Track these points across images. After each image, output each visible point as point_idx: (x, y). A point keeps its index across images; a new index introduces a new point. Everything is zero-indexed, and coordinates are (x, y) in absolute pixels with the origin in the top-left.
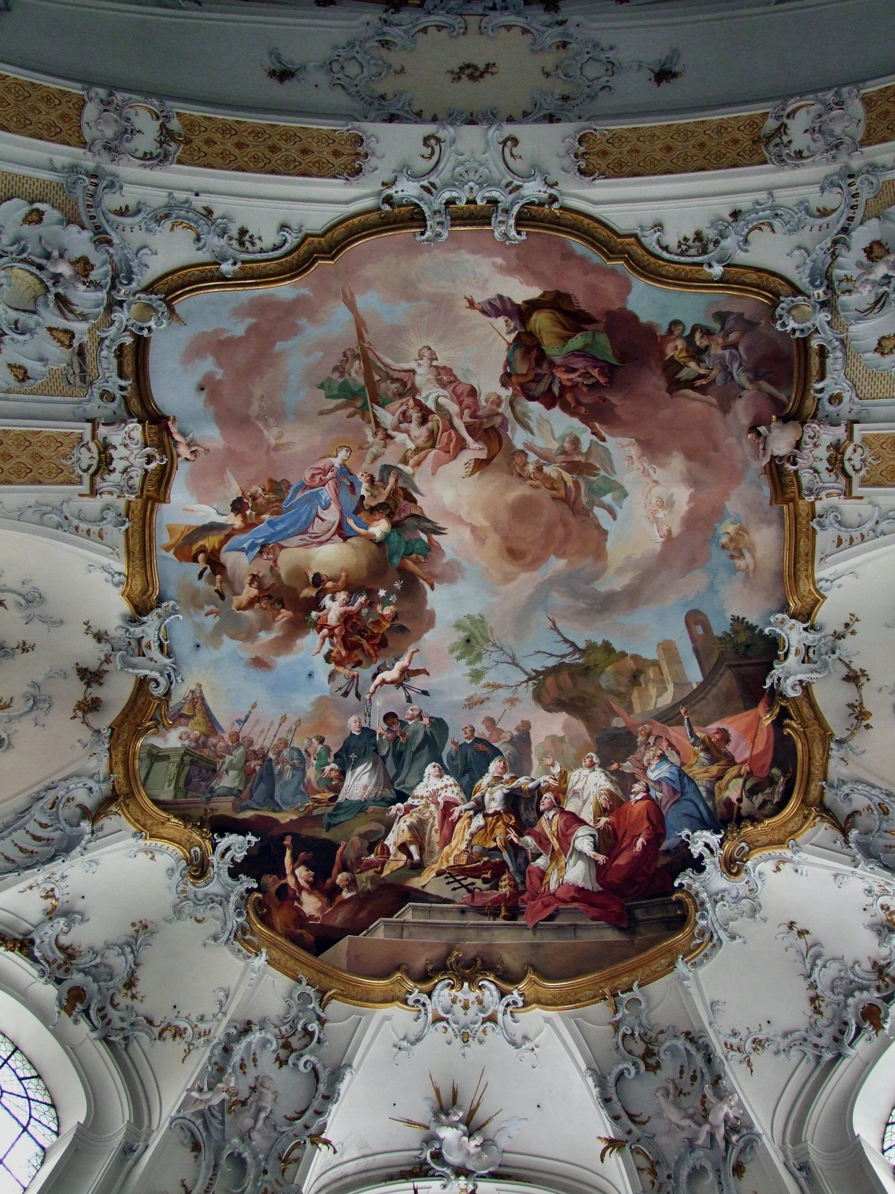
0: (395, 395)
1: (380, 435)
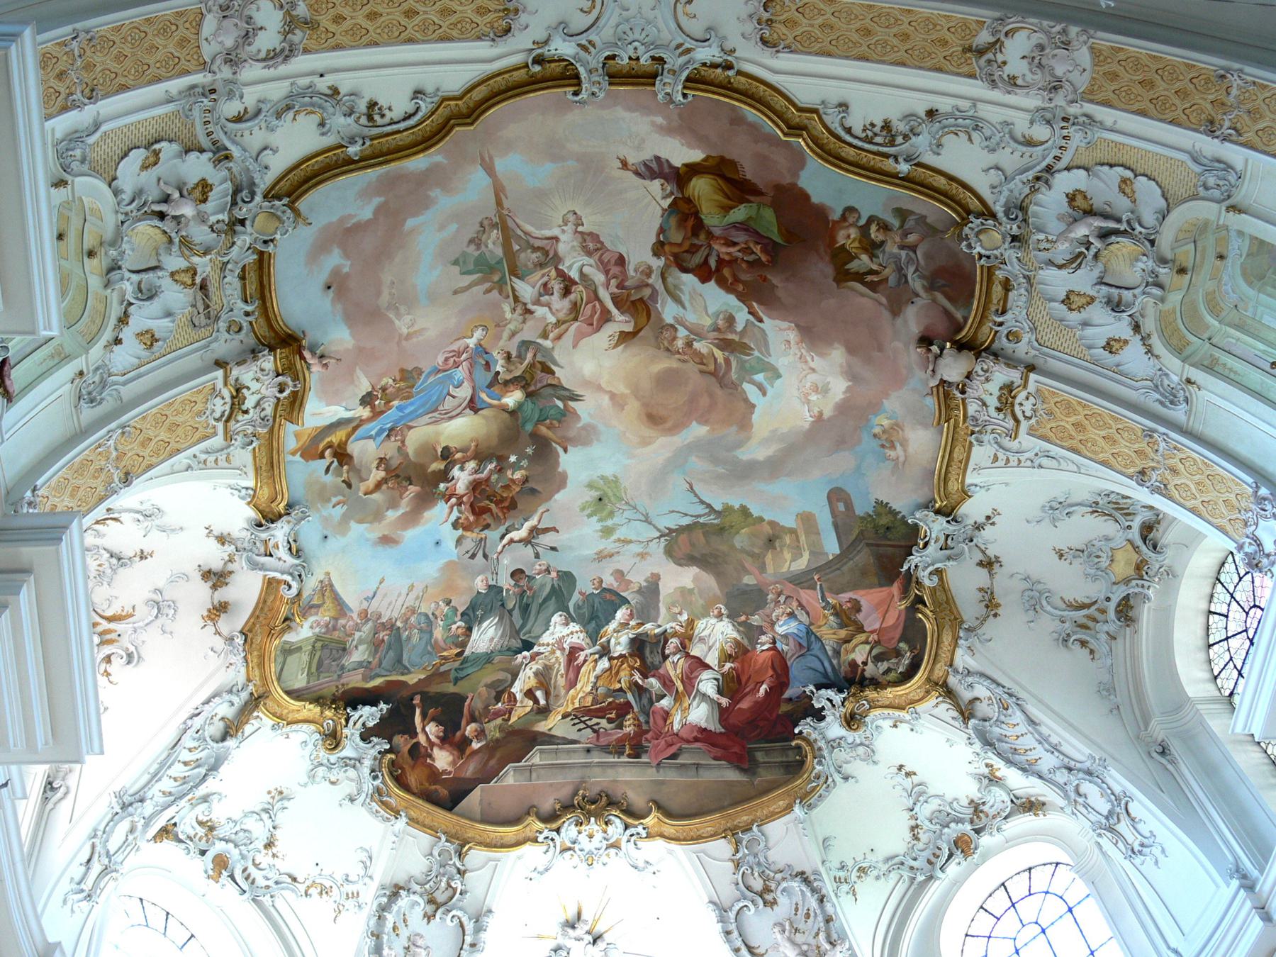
0: (535, 266)
1: (519, 310)
